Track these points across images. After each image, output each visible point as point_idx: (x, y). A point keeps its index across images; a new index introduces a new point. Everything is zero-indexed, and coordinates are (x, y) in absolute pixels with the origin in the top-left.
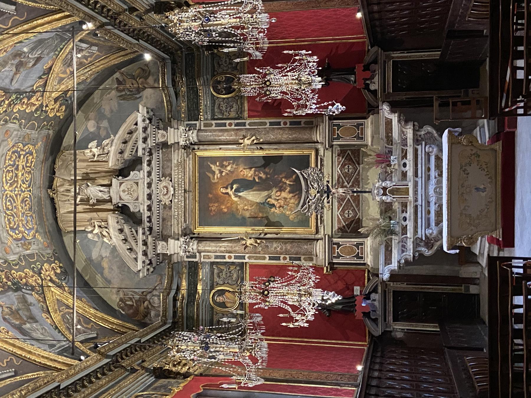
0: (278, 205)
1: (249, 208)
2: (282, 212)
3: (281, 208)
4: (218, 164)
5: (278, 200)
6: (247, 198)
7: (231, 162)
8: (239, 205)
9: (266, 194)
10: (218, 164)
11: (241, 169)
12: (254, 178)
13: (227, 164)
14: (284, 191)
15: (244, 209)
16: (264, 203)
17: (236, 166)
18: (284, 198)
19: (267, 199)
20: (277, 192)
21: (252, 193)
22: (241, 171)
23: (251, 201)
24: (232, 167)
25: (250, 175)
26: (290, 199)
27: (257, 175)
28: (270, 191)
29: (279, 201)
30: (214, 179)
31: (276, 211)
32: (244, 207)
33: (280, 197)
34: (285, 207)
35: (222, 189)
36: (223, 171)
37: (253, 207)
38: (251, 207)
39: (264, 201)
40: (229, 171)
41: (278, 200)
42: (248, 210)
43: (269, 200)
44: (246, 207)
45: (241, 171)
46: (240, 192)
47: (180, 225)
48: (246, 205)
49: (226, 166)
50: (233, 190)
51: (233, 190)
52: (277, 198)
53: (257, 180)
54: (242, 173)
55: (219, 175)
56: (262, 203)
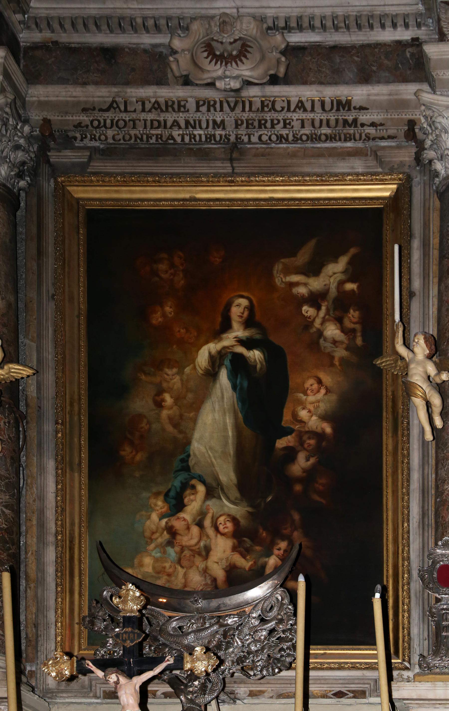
0: (178, 525)
1: (165, 413)
2: (152, 540)
3: (166, 536)
4: (350, 286)
5: (200, 524)
6: (207, 407)
7: (359, 341)
8: (181, 372)
9: (223, 479)
10: (350, 286)
11: (327, 379)
12: (288, 432)
13: (348, 324)
14: (234, 549)
15: (160, 392)
16: (187, 469)
17: (342, 359)
18: (208, 550)
19: (204, 482)
20: (234, 520)
21: (229, 421)
22: (320, 382)
23: (195, 420)
24: (335, 342)
25: (303, 414)
26: (205, 571)
27: (301, 443)
28: (235, 493)
29: (195, 530)
30: (288, 271)
31: (154, 517)
32: (170, 390)
33: (211, 532)
34: (172, 552)
35: (244, 302)
36: (318, 308)
37: (170, 428)
38: (170, 419)
39: (197, 471)
40: (320, 334)
41: (200, 524)
42: (159, 405)
43: (201, 489)
44: (168, 399)
45: (320, 382)
46: (232, 376)
47: (85, 118)
48: (177, 399)
49: (339, 321)
50: (240, 350)
51: (240, 350)
52: (207, 523)
53: (281, 443)
54: (311, 383)
55: (302, 290)
56: (185, 460)
